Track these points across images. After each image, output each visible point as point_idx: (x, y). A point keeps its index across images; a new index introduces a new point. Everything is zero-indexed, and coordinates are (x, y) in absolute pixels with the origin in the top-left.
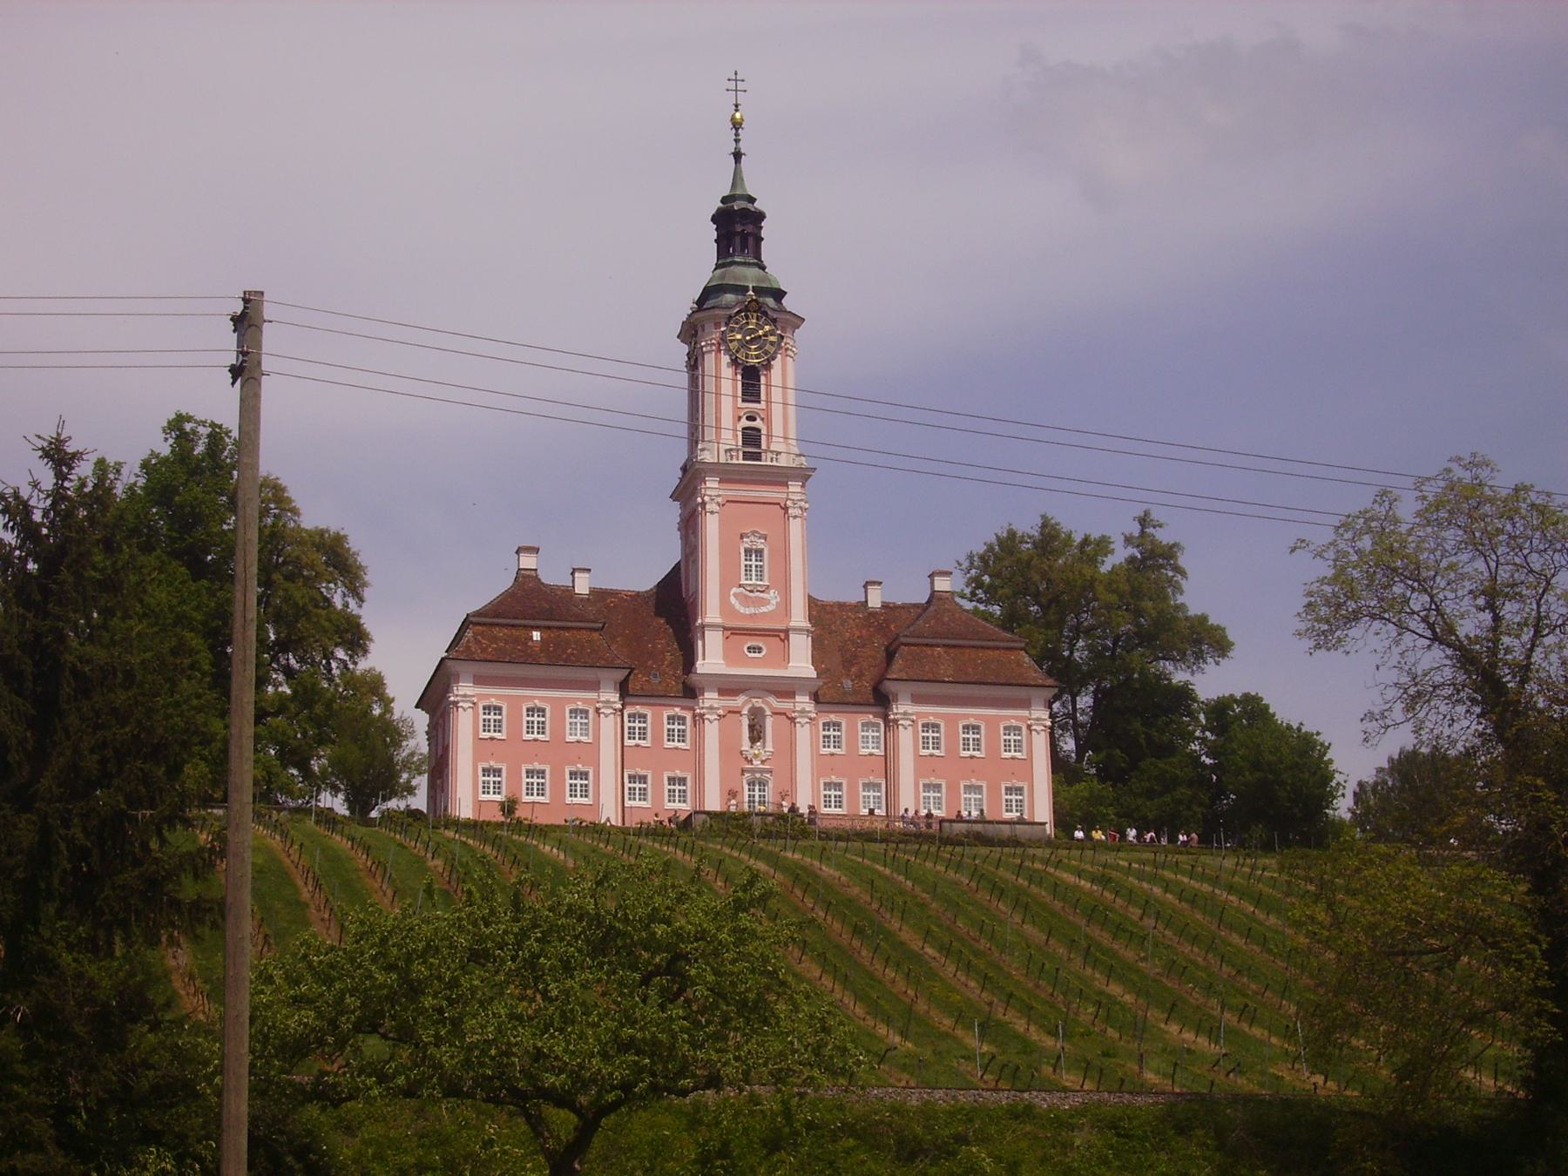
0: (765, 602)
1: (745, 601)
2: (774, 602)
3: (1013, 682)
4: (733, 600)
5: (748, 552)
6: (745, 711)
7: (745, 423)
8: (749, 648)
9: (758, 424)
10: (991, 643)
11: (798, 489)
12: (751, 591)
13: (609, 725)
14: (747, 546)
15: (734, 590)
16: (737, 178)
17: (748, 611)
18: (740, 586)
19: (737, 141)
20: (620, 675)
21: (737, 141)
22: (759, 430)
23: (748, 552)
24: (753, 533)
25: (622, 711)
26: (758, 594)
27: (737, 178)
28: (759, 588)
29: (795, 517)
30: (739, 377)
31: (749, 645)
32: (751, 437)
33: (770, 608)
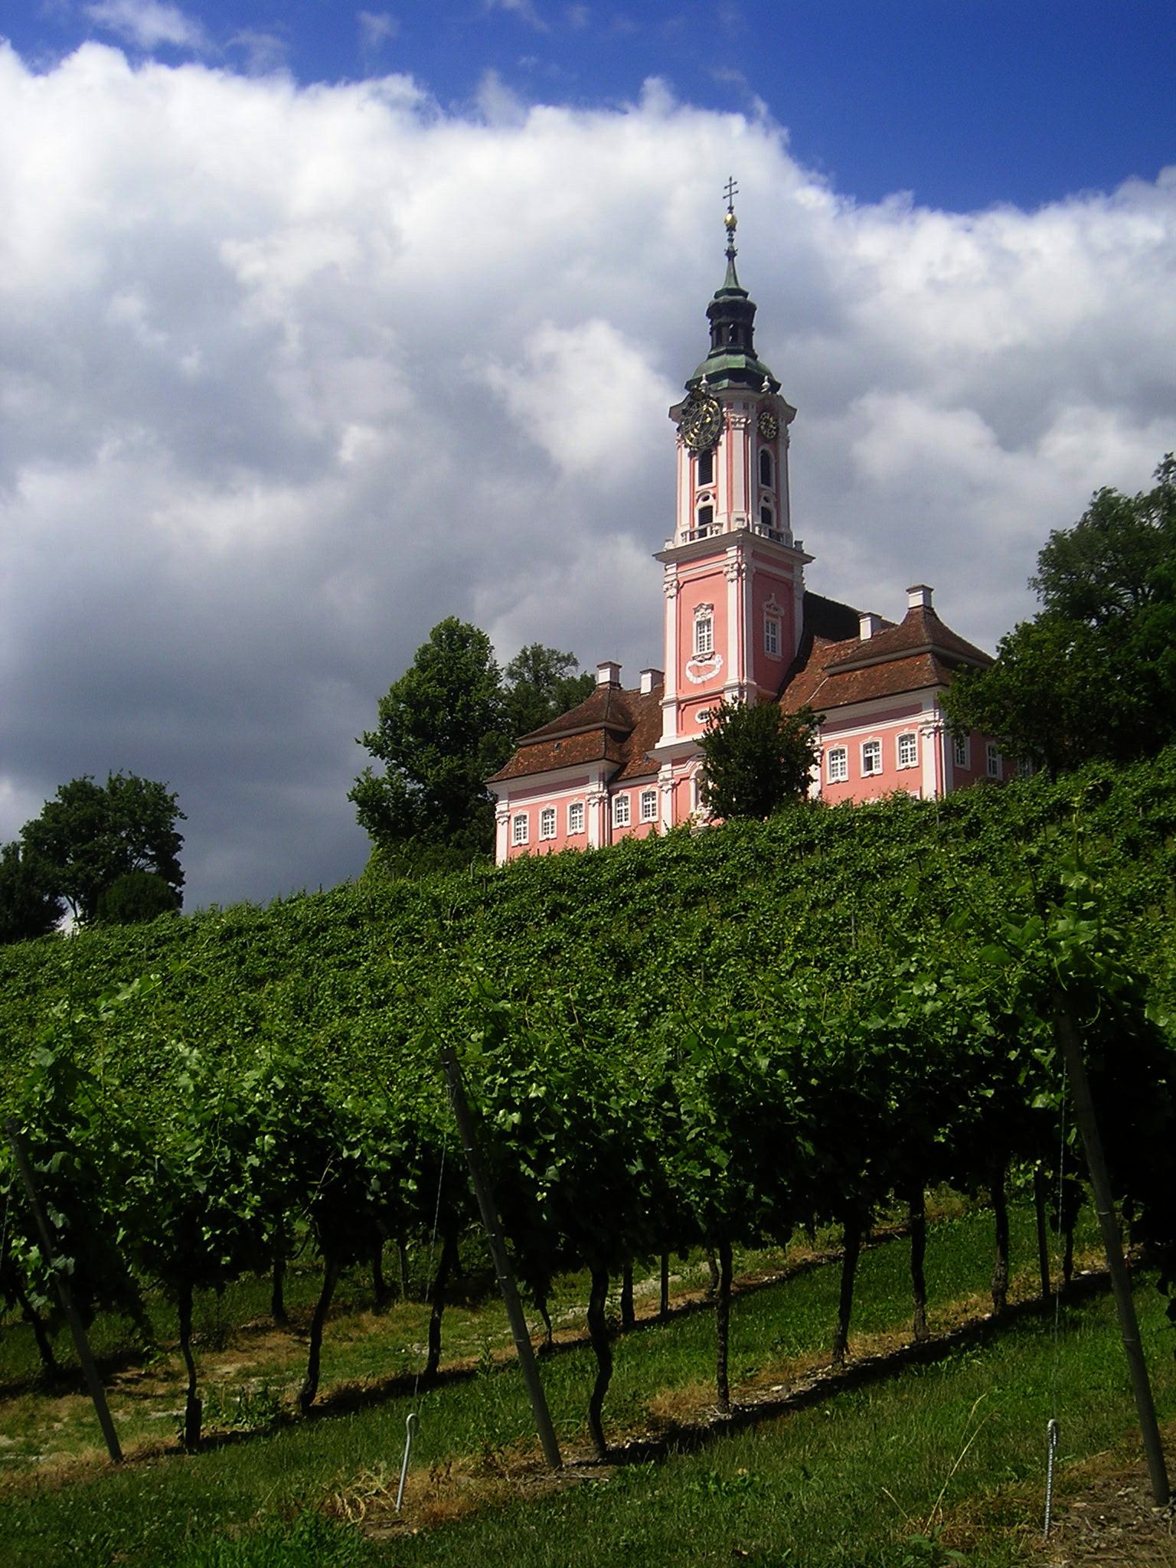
0: (710, 668)
1: (697, 671)
2: (718, 666)
3: (911, 687)
4: (688, 673)
5: (699, 624)
6: (693, 776)
7: (701, 504)
8: (702, 714)
9: (711, 502)
10: (895, 656)
11: (735, 553)
12: (701, 661)
13: (594, 813)
14: (698, 619)
15: (690, 664)
16: (732, 274)
17: (700, 680)
18: (694, 658)
19: (731, 240)
20: (602, 766)
21: (731, 240)
22: (711, 507)
23: (699, 624)
24: (701, 605)
25: (610, 798)
26: (707, 662)
27: (732, 274)
28: (707, 657)
29: (732, 580)
30: (697, 463)
31: (699, 712)
32: (706, 515)
33: (716, 672)
